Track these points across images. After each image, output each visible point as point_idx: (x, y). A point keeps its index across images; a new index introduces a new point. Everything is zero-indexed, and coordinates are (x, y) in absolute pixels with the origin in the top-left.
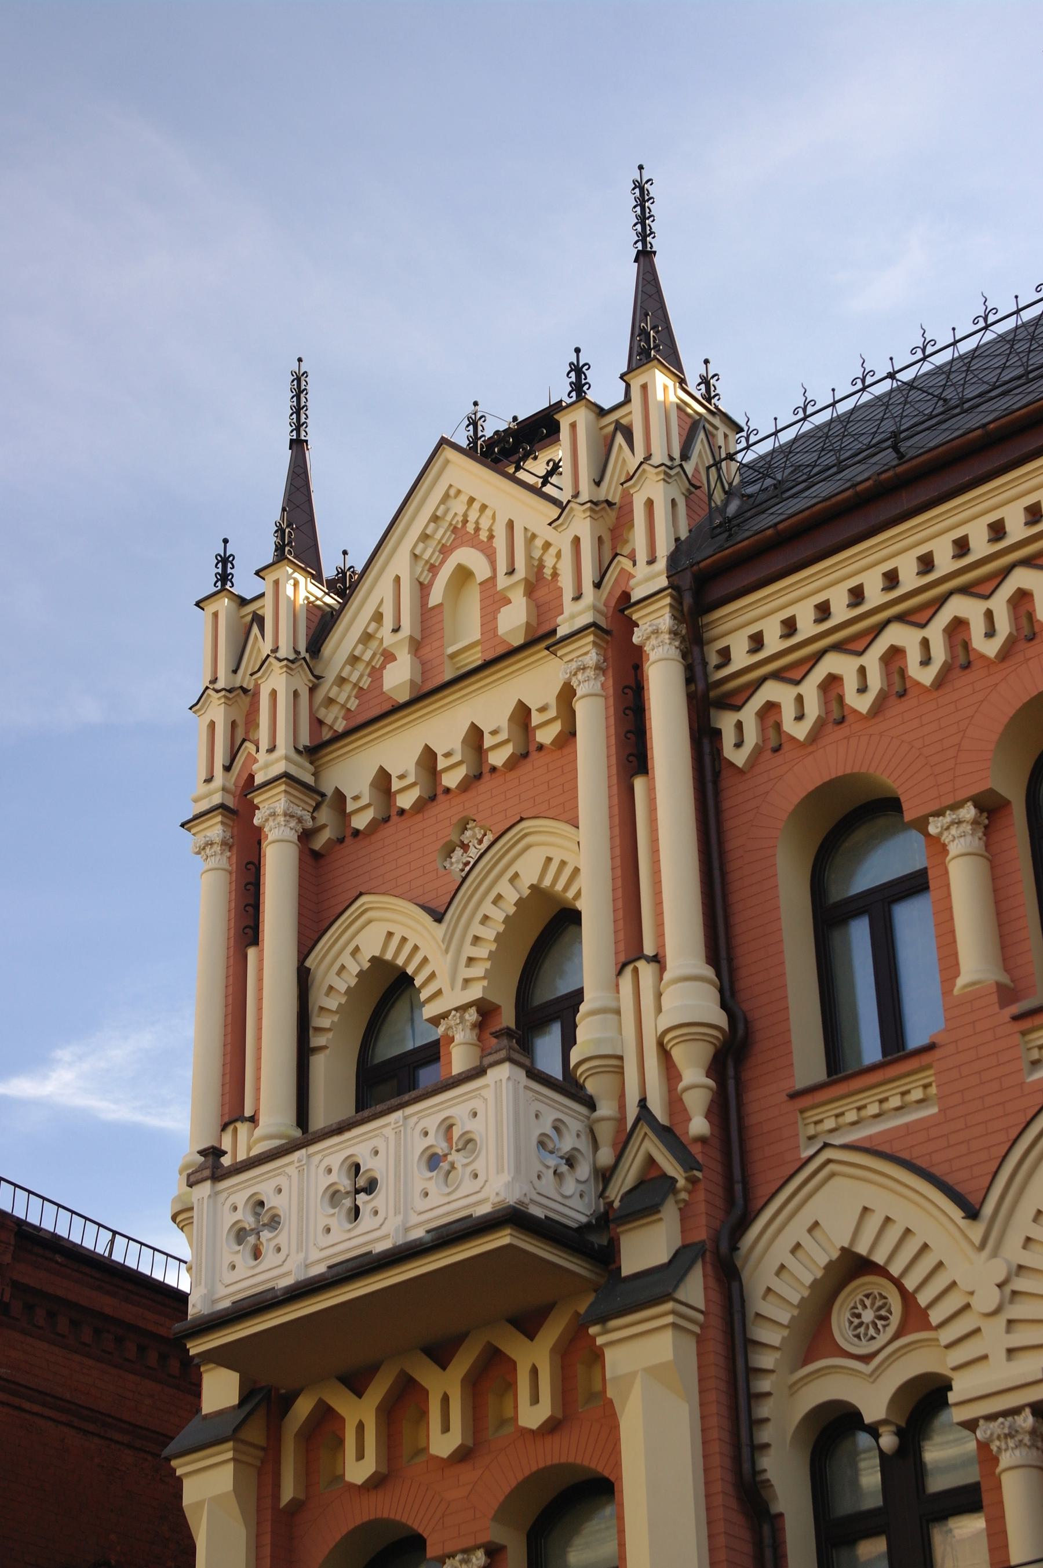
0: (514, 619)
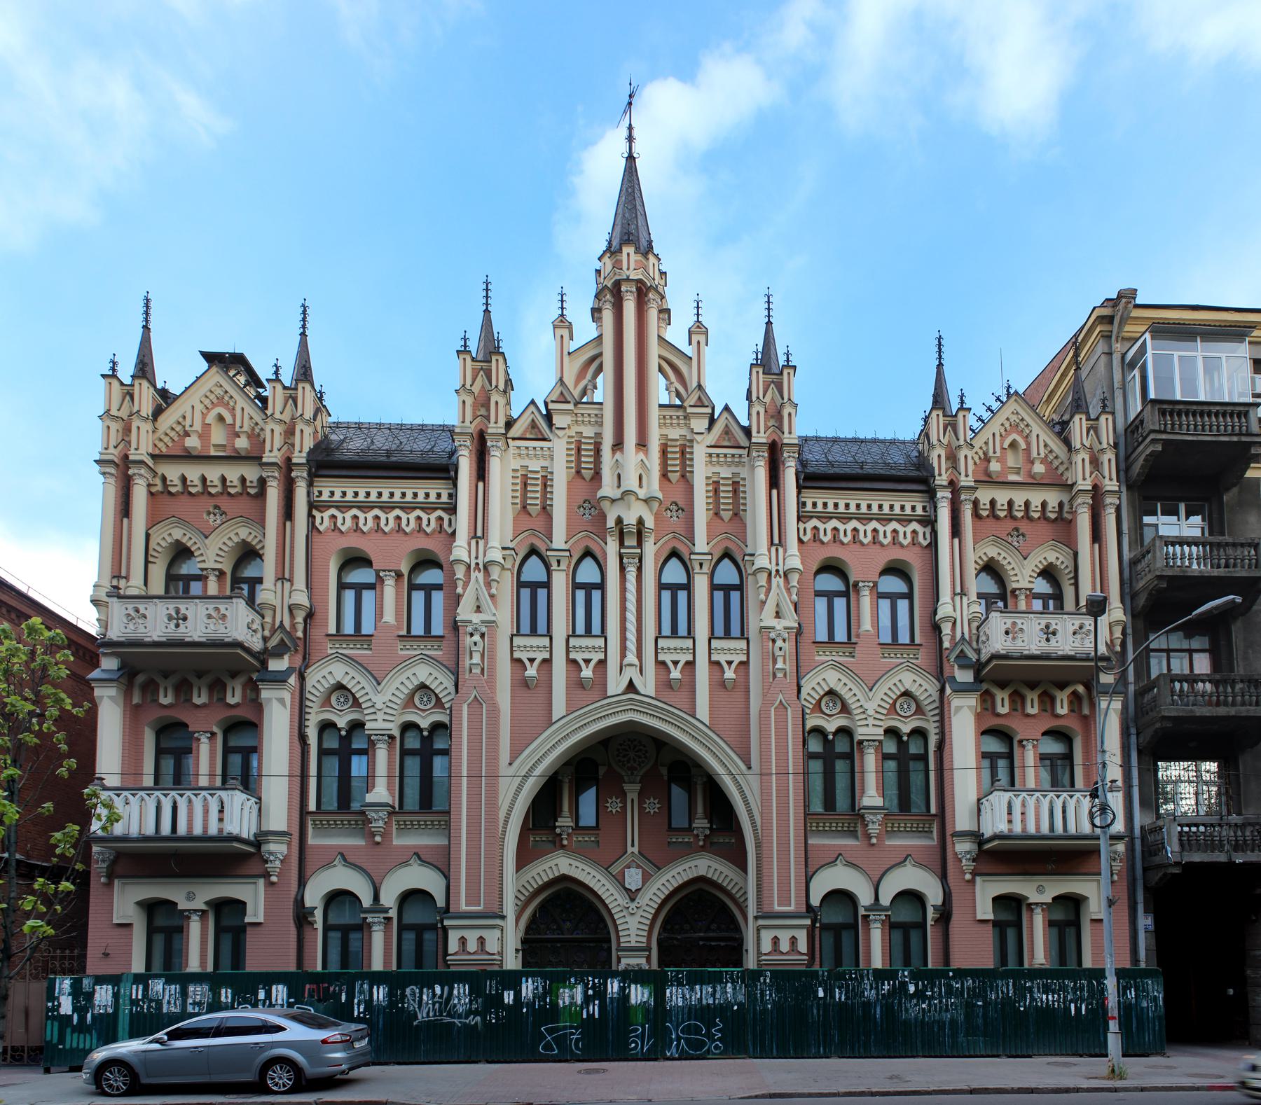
0: (242, 443)
